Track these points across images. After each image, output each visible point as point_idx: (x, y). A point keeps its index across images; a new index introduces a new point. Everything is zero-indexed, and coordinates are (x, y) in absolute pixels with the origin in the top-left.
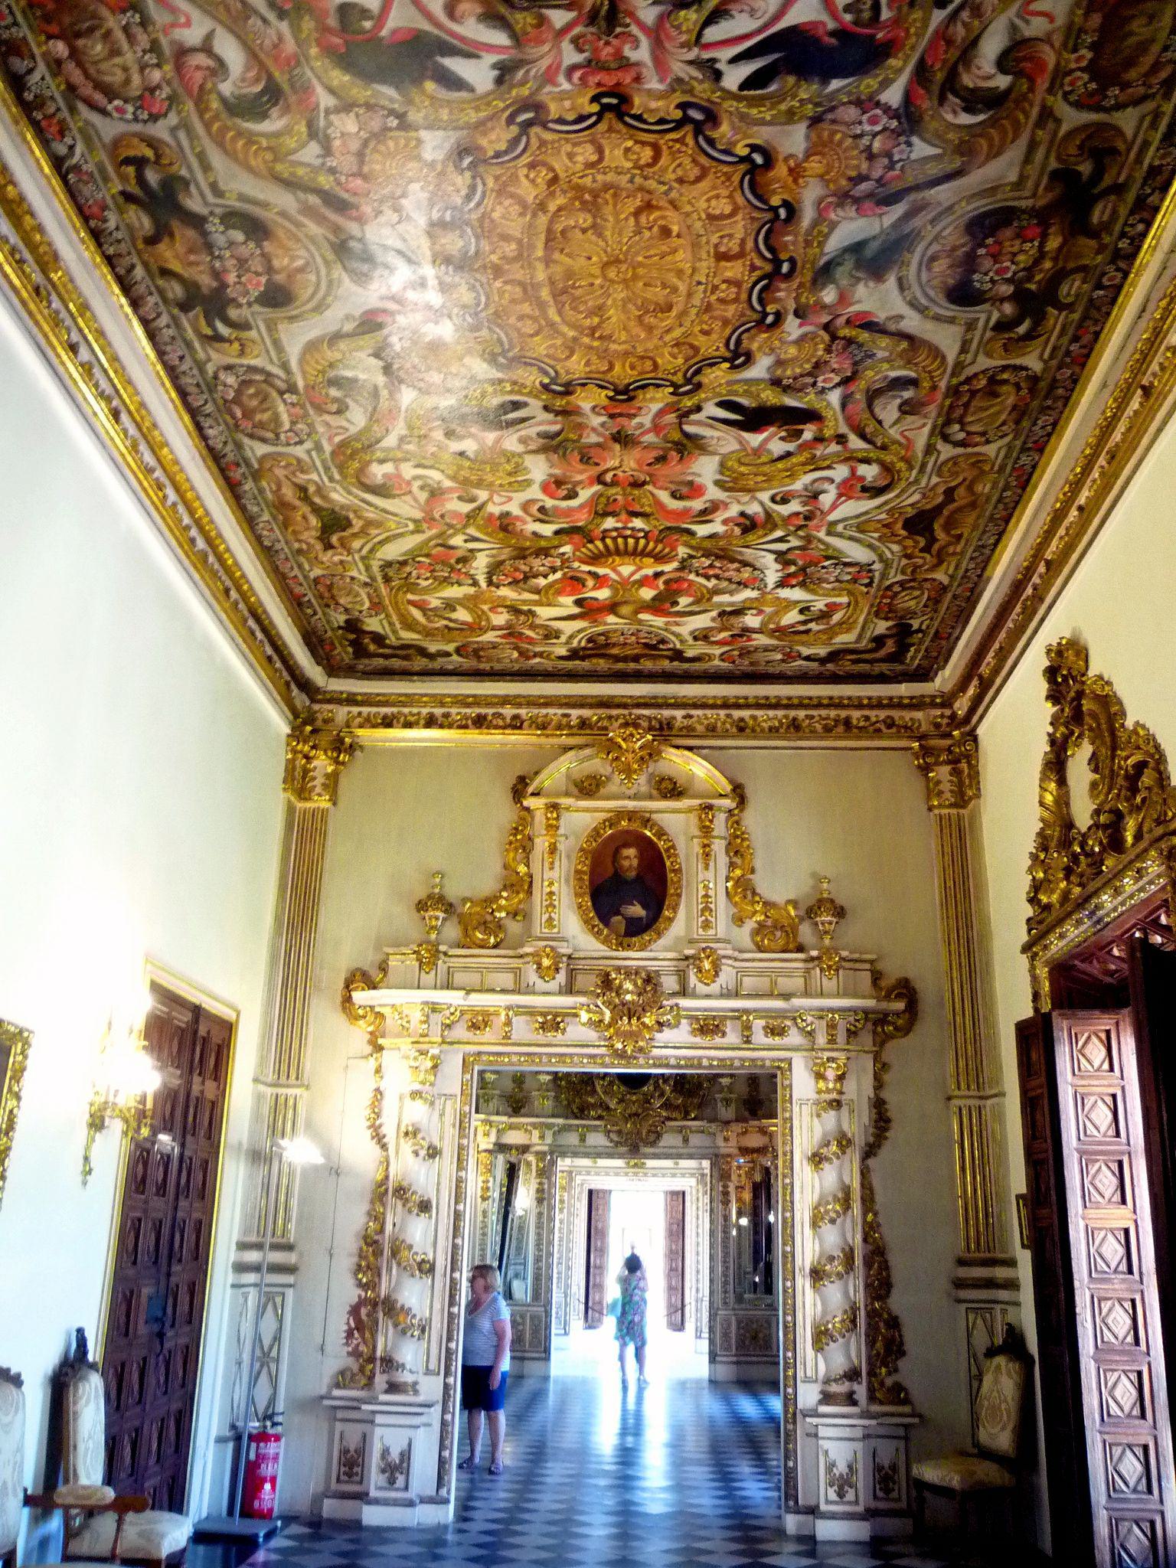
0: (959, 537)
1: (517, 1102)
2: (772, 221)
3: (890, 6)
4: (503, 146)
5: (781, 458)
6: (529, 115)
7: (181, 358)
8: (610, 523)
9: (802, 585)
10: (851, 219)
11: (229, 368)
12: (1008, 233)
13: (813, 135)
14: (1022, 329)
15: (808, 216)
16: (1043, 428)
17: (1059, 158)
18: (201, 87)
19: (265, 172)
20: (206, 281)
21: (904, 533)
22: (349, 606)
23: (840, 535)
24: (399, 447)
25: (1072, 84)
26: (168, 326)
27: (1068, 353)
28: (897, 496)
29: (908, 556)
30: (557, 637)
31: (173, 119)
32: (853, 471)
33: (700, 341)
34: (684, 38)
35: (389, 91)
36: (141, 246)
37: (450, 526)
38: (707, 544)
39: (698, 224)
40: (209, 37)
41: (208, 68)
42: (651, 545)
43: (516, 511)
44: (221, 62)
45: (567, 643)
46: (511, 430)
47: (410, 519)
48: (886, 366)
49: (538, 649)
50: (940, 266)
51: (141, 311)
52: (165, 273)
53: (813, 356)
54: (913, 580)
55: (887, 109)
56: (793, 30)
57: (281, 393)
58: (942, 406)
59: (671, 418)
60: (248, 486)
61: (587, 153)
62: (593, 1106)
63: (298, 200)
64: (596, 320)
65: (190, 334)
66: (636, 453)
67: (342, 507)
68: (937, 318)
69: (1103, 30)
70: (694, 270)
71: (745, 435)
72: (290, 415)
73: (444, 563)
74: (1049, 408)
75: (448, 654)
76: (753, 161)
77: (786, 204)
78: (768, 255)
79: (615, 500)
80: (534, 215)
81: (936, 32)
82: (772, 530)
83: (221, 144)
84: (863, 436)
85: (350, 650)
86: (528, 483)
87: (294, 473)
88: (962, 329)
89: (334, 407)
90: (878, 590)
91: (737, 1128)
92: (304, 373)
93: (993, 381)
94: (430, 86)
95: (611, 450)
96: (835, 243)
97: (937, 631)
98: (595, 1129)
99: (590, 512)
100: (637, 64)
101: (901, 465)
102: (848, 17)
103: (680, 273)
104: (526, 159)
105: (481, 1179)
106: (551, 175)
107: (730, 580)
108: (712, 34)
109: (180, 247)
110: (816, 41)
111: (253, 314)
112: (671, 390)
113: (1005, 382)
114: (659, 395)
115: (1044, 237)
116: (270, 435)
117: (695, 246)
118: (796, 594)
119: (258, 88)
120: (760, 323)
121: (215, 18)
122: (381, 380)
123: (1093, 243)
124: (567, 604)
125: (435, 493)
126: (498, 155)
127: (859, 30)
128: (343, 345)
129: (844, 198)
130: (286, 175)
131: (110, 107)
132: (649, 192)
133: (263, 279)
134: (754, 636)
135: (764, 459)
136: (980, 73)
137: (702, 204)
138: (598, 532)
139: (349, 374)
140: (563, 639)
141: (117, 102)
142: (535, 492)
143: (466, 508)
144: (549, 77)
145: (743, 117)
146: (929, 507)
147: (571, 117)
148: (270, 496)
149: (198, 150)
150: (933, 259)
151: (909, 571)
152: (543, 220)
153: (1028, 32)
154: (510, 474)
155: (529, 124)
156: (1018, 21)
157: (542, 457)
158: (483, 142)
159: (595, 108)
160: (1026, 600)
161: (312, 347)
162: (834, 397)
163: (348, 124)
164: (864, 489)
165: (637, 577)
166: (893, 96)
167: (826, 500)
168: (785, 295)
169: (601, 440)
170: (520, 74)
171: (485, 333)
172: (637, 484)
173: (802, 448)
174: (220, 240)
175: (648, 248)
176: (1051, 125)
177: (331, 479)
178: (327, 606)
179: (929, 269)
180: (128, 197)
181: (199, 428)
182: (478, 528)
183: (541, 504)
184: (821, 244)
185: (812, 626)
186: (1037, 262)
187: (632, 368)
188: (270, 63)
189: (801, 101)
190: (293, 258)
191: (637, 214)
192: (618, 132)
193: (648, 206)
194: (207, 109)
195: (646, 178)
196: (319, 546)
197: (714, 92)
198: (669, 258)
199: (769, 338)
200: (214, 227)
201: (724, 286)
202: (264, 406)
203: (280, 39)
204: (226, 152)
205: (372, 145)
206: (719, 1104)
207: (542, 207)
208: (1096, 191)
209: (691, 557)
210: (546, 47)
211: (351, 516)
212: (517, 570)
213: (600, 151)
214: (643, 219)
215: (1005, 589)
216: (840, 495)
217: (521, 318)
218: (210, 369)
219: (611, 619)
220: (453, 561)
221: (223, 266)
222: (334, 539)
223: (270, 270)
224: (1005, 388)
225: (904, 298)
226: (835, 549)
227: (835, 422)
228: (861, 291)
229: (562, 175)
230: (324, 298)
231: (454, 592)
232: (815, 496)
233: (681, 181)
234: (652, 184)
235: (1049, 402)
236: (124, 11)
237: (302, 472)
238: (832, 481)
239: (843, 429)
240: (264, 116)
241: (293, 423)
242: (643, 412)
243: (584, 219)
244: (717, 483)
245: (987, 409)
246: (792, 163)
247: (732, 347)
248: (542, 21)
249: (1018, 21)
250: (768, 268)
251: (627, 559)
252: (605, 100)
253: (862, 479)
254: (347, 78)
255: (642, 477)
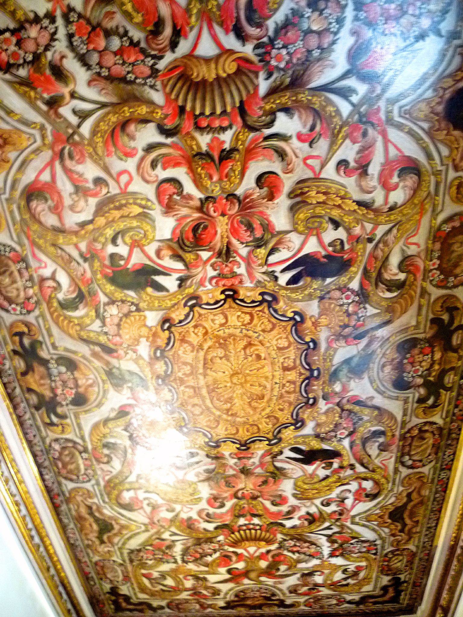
0: (417, 522)
2: (306, 350)
3: (348, 243)
4: (182, 317)
5: (324, 479)
6: (194, 301)
7: (35, 436)
8: (242, 521)
9: (342, 555)
10: (344, 347)
11: (56, 440)
12: (416, 351)
13: (322, 307)
14: (431, 402)
15: (323, 346)
16: (449, 456)
17: (433, 313)
18: (50, 297)
19: (76, 336)
20: (48, 394)
21: (389, 521)
22: (112, 579)
23: (357, 524)
24: (137, 481)
25: (433, 276)
26: (29, 419)
27: (454, 414)
28: (383, 499)
29: (393, 535)
30: (219, 595)
31: (37, 312)
32: (360, 484)
33: (279, 414)
34: (260, 262)
35: (131, 293)
36: (19, 376)
37: (163, 527)
38: (292, 532)
39: (274, 352)
40: (54, 273)
41: (53, 287)
42: (264, 533)
43: (195, 516)
44: (59, 284)
45: (225, 598)
46: (191, 468)
47: (142, 524)
48: (369, 424)
49: (210, 603)
50: (388, 369)
51: (18, 411)
52: (30, 390)
53: (333, 421)
54: (398, 550)
55: (353, 291)
56: (307, 256)
57: (80, 453)
58: (398, 446)
59: (268, 458)
60: (64, 507)
61: (220, 319)
63: (91, 350)
64: (229, 405)
65: (39, 423)
66: (253, 479)
67: (110, 518)
68: (390, 398)
69: (441, 249)
70: (273, 376)
71: (306, 467)
72: (85, 465)
73: (159, 549)
74: (450, 445)
75: (162, 608)
76: (295, 319)
77: (313, 341)
78: (307, 367)
79: (244, 507)
80: (198, 351)
81: (370, 254)
82: (323, 522)
83: (57, 323)
84: (362, 465)
85: (112, 607)
86: (200, 499)
87: (85, 499)
88: (402, 403)
89: (105, 460)
90: (381, 557)
92: (91, 440)
93: (421, 431)
94: (149, 290)
95: (240, 478)
96: (338, 359)
97: (414, 582)
99: (231, 515)
100: (240, 275)
101: (383, 481)
102: (330, 249)
103: (266, 378)
104: (193, 323)
106: (204, 331)
107: (304, 553)
108: (273, 259)
109: (37, 377)
110: (318, 260)
111: (68, 410)
112: (267, 442)
113: (426, 431)
114: (261, 446)
115: (433, 352)
116: (75, 477)
117: (273, 364)
118: (339, 561)
119: (74, 295)
120: (307, 403)
121: (57, 263)
122: (128, 443)
123: (455, 355)
124: (223, 573)
125: (155, 508)
126: (180, 322)
127: (336, 254)
128: (110, 425)
129: (339, 336)
130: (85, 337)
131: (10, 308)
132: (250, 337)
133: (74, 391)
134: (321, 589)
135: (316, 480)
136: (392, 272)
137: (274, 342)
138: (236, 528)
139: (112, 440)
140: (222, 595)
141: (13, 306)
142: (203, 505)
143: (170, 515)
144: (201, 283)
145: (289, 298)
146: (400, 504)
147: (212, 302)
148: (74, 513)
149: (47, 326)
150: (384, 366)
151: (395, 544)
152: (202, 354)
153: (410, 253)
154: (192, 495)
155: (193, 306)
156: (405, 248)
157: (206, 484)
158: (173, 316)
159: (223, 297)
160: (459, 555)
161: (96, 426)
162: (346, 443)
163: (113, 310)
164: (367, 496)
165: (257, 554)
166: (355, 285)
167: (349, 502)
168: (317, 388)
169: (234, 472)
170: (189, 282)
171: (176, 415)
172: (255, 498)
173: (335, 471)
174: (55, 371)
175: (251, 366)
176: (427, 297)
177: (104, 501)
178: (101, 579)
179: (383, 371)
180: (15, 352)
181: (41, 474)
182: (178, 528)
183: (207, 511)
184: (331, 360)
185: (350, 581)
186: (432, 365)
187: (248, 431)
188: (80, 284)
189: (314, 289)
190: (87, 379)
191: (245, 348)
192: (234, 308)
193: (250, 344)
194: (52, 307)
195: (248, 330)
196: (97, 542)
197: (275, 287)
198: (261, 371)
199: (311, 412)
200: (52, 365)
201: (288, 384)
202: (73, 460)
203: (85, 272)
204: (60, 328)
205: (124, 319)
207: (201, 347)
208: (452, 328)
209: (285, 540)
210: (200, 269)
211: (113, 523)
212: (197, 552)
213: (226, 318)
214: (248, 351)
215: (446, 552)
216: (356, 499)
217: (194, 405)
218: (48, 441)
219: (246, 581)
220: (164, 548)
221: (56, 386)
222: (105, 537)
223: (77, 386)
224: (428, 435)
225: (373, 387)
226: (356, 532)
227: (349, 458)
228: (353, 384)
229: (210, 331)
230: (101, 400)
231: (165, 567)
232: (342, 501)
233: (264, 331)
234: (250, 333)
235: (449, 442)
236: (19, 262)
237: (90, 497)
238: (350, 491)
239: (353, 461)
240: (76, 308)
241: (86, 470)
242: (254, 456)
243: (220, 352)
244: (294, 495)
245: (420, 446)
246: (313, 320)
247: (295, 417)
248: (198, 256)
249: (405, 248)
250: (308, 374)
251: (252, 543)
252: (227, 293)
253: (365, 489)
254: (113, 288)
255: (257, 493)
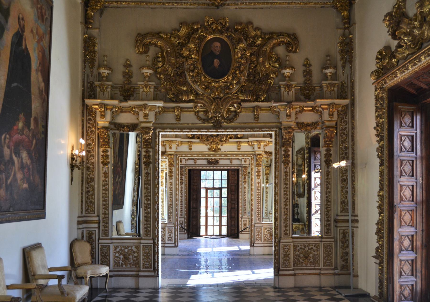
1: (128, 90)
62: (187, 93)
91: (297, 106)
98: (188, 109)
105: (101, 149)
206: (283, 89)
